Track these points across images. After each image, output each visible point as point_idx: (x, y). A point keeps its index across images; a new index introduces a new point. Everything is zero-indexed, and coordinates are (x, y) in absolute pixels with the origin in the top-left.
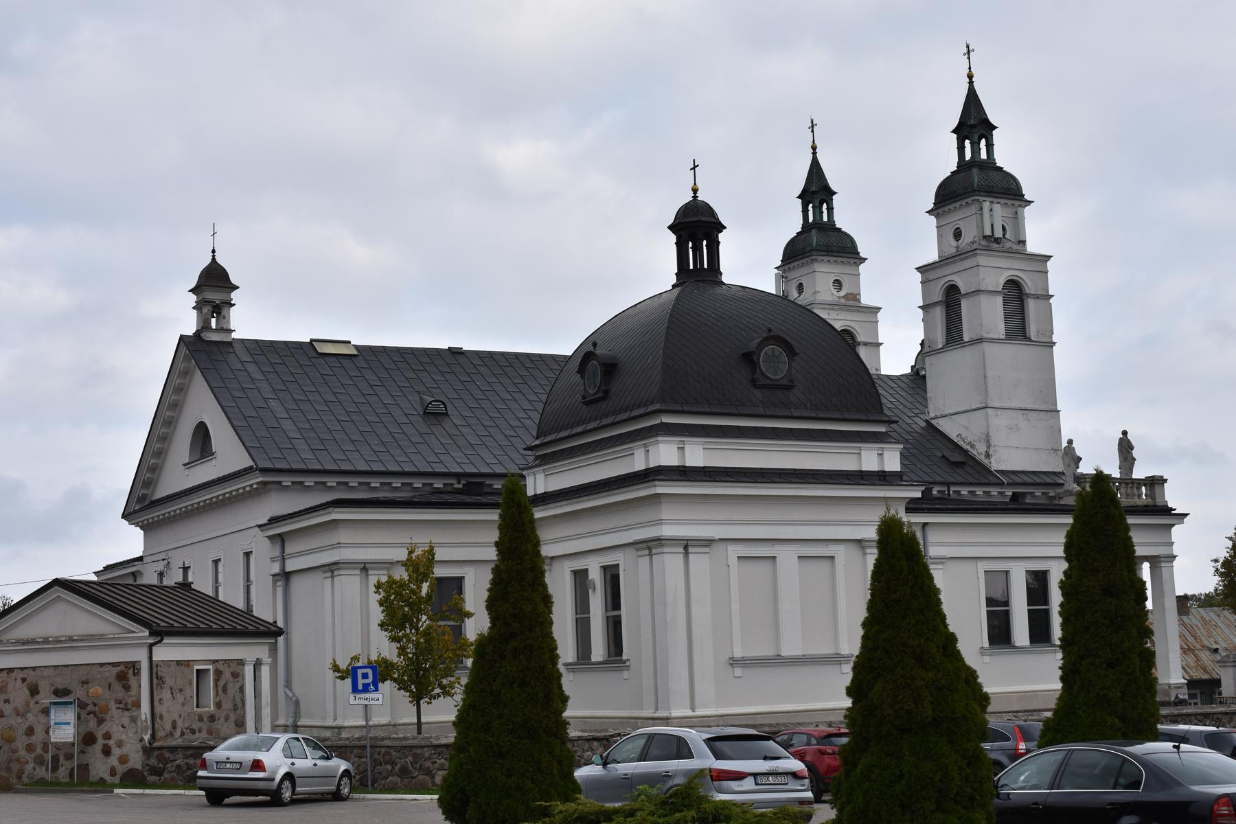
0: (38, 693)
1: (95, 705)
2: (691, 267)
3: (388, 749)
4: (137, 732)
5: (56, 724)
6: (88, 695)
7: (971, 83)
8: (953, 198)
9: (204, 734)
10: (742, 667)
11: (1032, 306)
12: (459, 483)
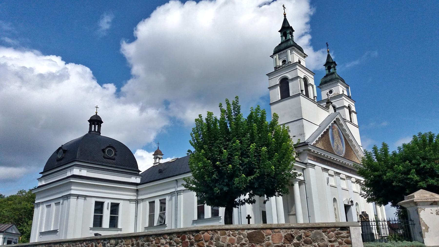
2: (93, 130)
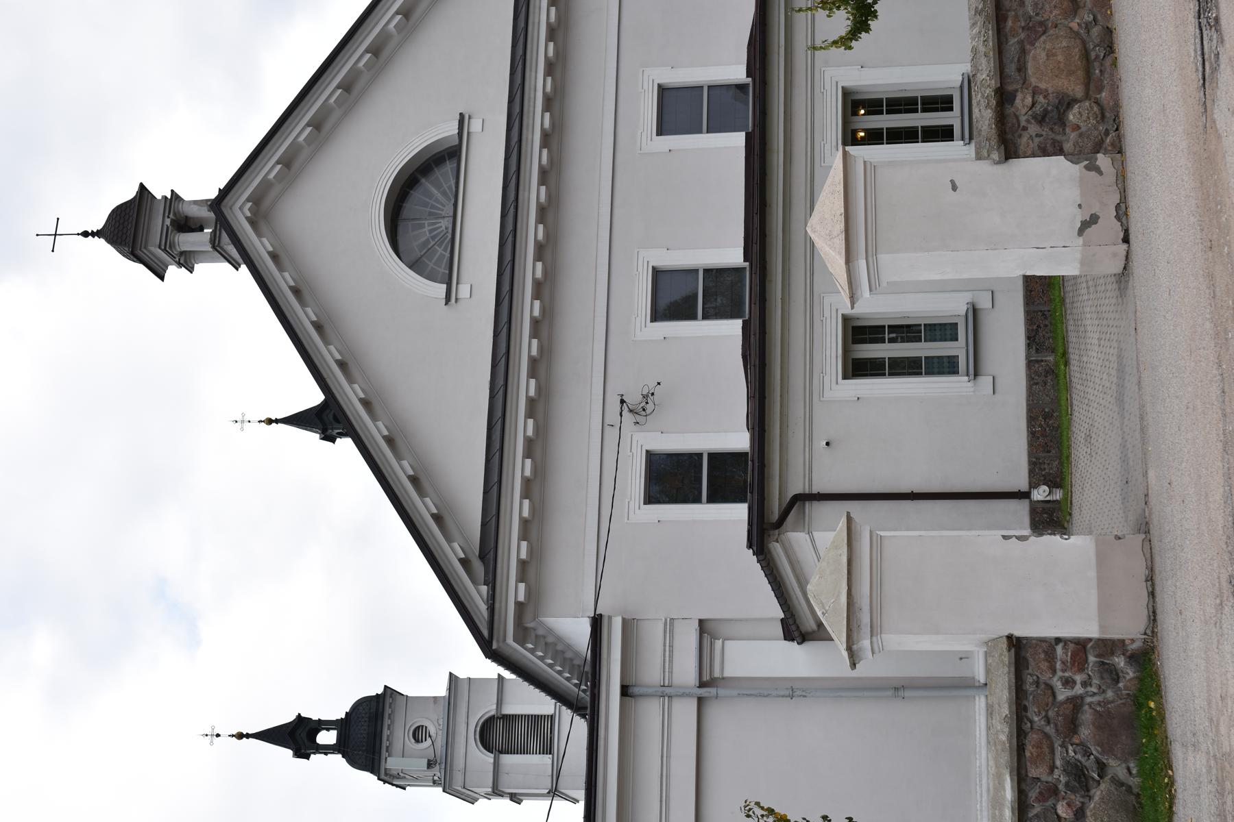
7: (277, 421)
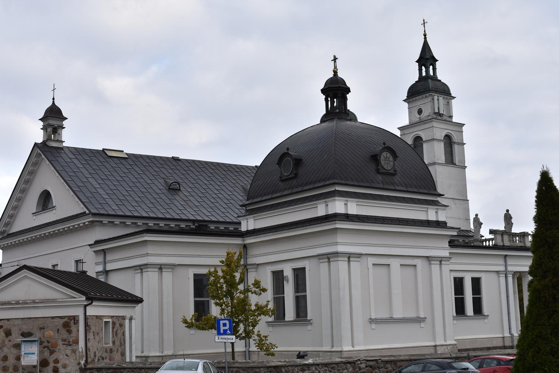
0: (11, 334)
1: (48, 342)
3: (238, 369)
4: (76, 358)
5: (25, 354)
6: (44, 336)
7: (425, 38)
8: (417, 94)
9: (107, 361)
10: (375, 324)
11: (456, 148)
12: (194, 225)
